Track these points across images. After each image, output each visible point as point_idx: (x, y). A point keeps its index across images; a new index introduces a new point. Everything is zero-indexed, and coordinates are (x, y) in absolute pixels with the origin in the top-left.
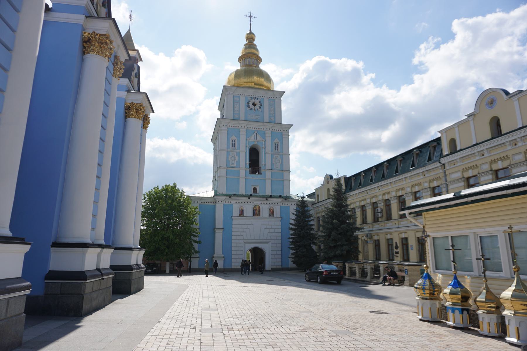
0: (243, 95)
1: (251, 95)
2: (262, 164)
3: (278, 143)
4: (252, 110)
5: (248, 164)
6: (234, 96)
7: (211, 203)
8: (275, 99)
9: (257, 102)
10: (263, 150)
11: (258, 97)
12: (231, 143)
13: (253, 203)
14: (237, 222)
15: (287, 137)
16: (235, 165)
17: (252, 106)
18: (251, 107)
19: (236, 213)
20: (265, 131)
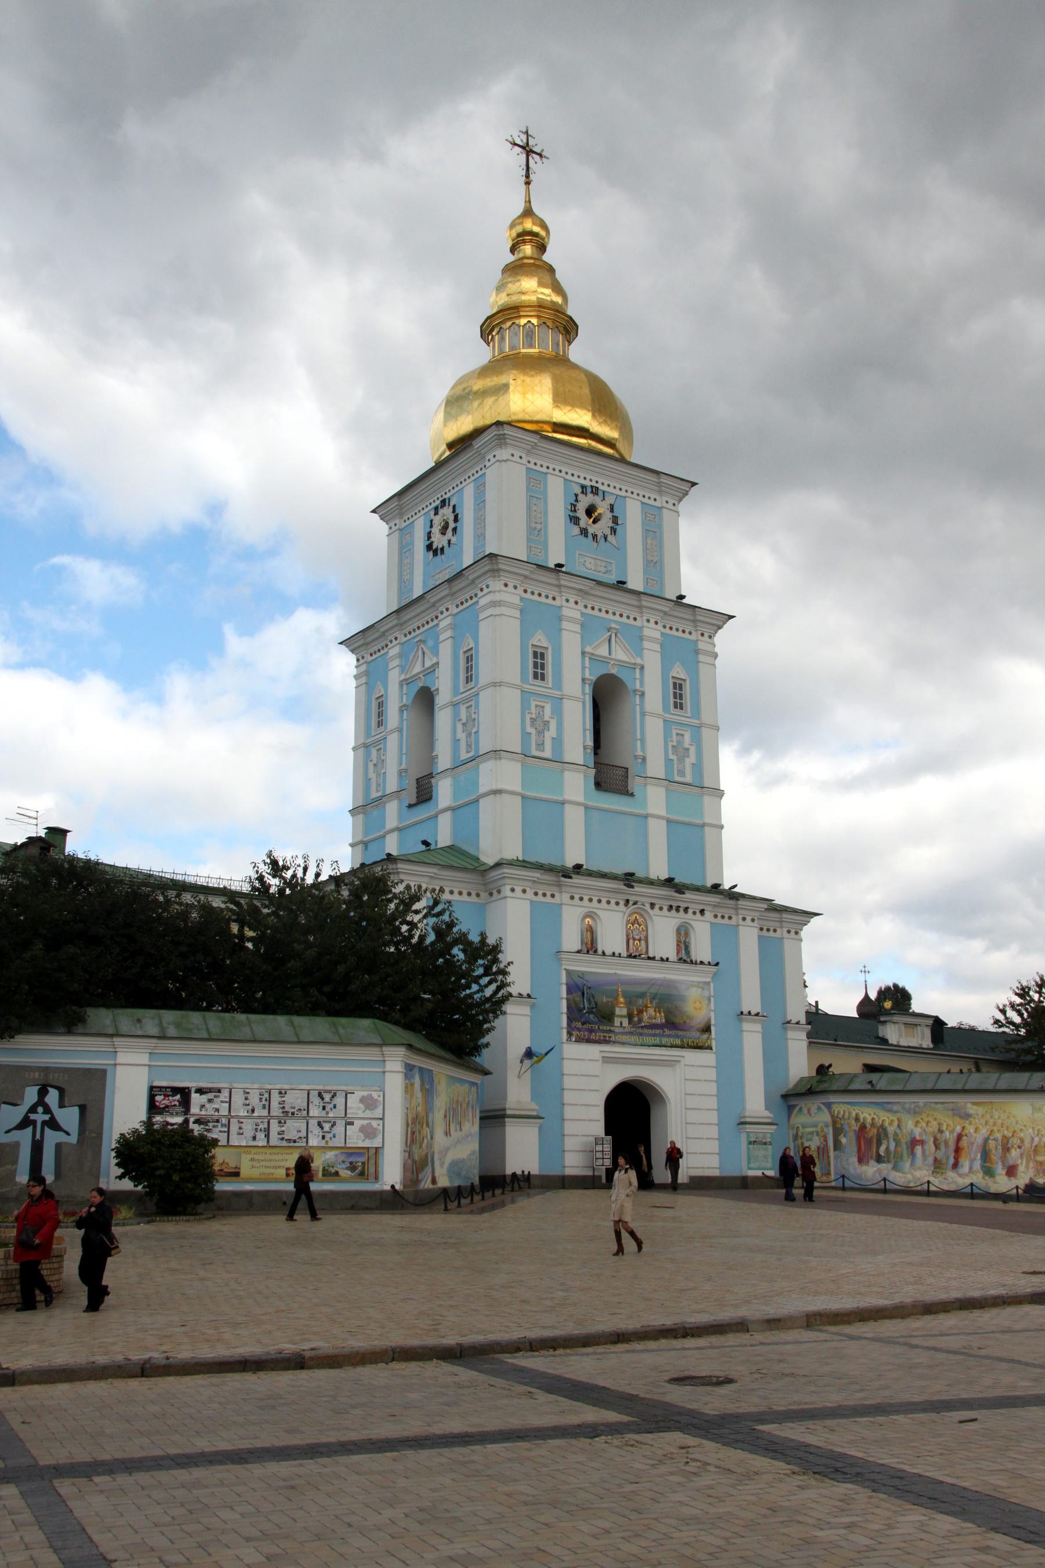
0: (557, 472)
1: (582, 476)
2: (636, 757)
3: (684, 680)
5: (589, 751)
10: (638, 702)
11: (604, 488)
12: (531, 660)
15: (709, 660)
16: (547, 753)
17: (584, 520)
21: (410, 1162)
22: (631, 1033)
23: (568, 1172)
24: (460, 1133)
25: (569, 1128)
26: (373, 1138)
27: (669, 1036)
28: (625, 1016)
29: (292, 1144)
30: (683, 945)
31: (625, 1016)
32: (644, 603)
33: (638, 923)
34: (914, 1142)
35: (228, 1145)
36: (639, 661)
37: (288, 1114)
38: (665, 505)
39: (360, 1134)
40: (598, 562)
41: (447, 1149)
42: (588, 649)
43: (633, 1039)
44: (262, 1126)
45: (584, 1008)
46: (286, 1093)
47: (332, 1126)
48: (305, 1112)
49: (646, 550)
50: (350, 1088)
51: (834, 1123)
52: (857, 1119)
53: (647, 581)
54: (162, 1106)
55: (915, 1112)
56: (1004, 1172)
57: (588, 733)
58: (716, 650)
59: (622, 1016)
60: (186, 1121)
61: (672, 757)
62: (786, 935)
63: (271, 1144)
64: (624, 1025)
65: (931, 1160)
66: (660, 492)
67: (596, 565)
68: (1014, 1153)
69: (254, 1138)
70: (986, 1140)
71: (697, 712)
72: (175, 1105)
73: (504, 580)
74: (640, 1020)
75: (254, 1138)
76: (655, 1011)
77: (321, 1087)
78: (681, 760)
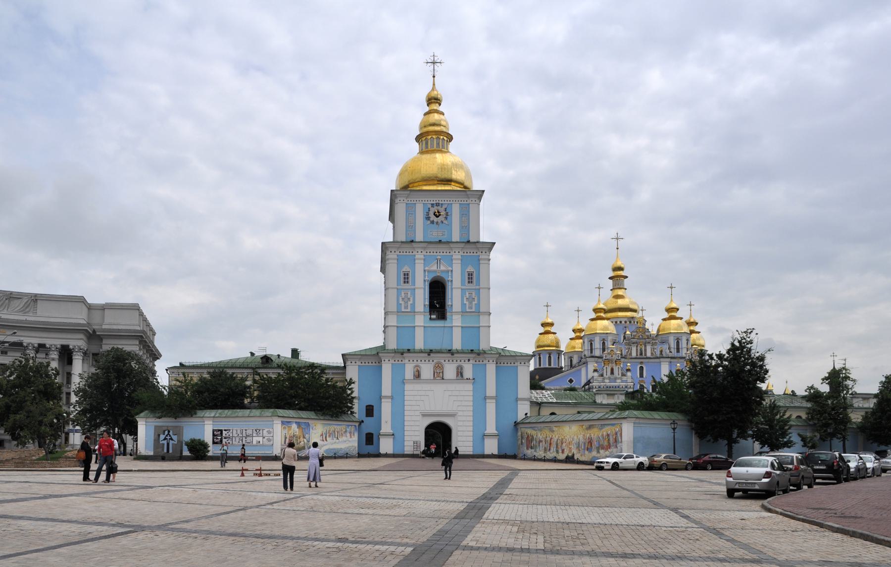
0: (421, 202)
2: (448, 305)
3: (473, 272)
4: (433, 223)
6: (406, 204)
7: (375, 363)
8: (469, 204)
9: (442, 210)
10: (450, 284)
11: (443, 202)
12: (402, 276)
13: (433, 361)
14: (411, 389)
15: (487, 262)
17: (433, 218)
18: (431, 219)
19: (409, 373)
20: (452, 256)
23: (406, 453)
24: (338, 441)
25: (406, 438)
30: (460, 373)
32: (451, 246)
34: (540, 441)
35: (232, 444)
36: (450, 269)
37: (247, 436)
38: (471, 202)
40: (439, 232)
42: (426, 268)
49: (461, 222)
50: (264, 428)
51: (521, 435)
52: (527, 433)
53: (461, 235)
55: (541, 430)
56: (561, 452)
57: (427, 300)
58: (491, 257)
61: (465, 302)
62: (519, 364)
65: (544, 447)
66: (469, 198)
67: (437, 234)
68: (564, 445)
70: (557, 440)
71: (478, 283)
73: (390, 250)
78: (471, 303)
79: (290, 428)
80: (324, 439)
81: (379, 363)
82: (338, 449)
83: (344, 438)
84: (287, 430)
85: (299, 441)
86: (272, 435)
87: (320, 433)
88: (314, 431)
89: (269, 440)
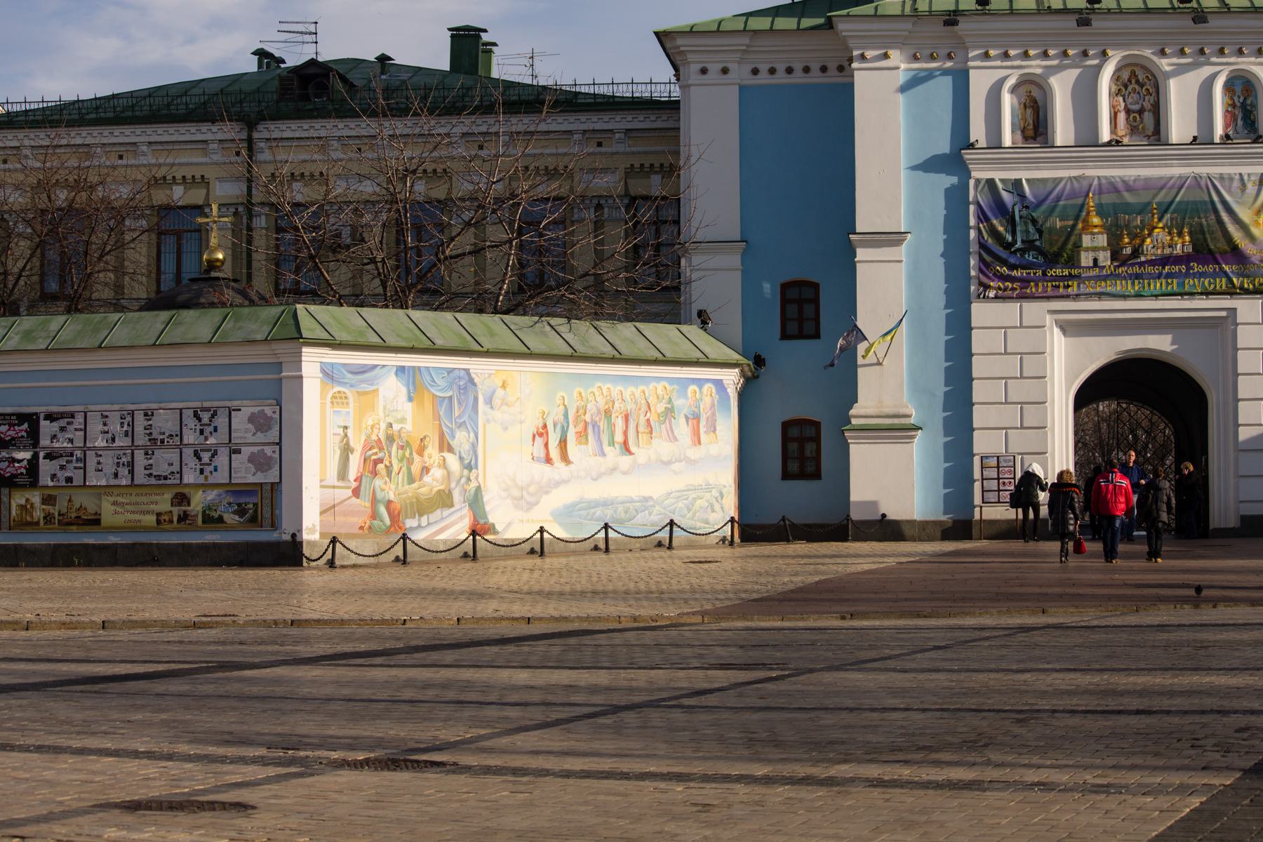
21: (363, 503)
22: (1118, 276)
24: (625, 461)
26: (266, 471)
27: (1201, 275)
28: (1103, 249)
29: (162, 482)
31: (1103, 249)
33: (1137, 82)
37: (155, 443)
39: (250, 465)
41: (558, 484)
43: (1119, 287)
44: (124, 460)
45: (1015, 242)
46: (152, 415)
47: (213, 456)
48: (178, 438)
50: (236, 403)
54: (7, 439)
59: (1095, 249)
60: (35, 456)
63: (136, 482)
64: (1101, 263)
69: (116, 475)
72: (23, 437)
74: (1136, 252)
75: (116, 475)
76: (1170, 233)
77: (198, 404)
79: (368, 398)
80: (554, 453)
81: (841, 68)
82: (632, 501)
83: (661, 447)
84: (351, 409)
85: (416, 468)
86: (273, 435)
87: (532, 424)
88: (497, 414)
89: (260, 462)
